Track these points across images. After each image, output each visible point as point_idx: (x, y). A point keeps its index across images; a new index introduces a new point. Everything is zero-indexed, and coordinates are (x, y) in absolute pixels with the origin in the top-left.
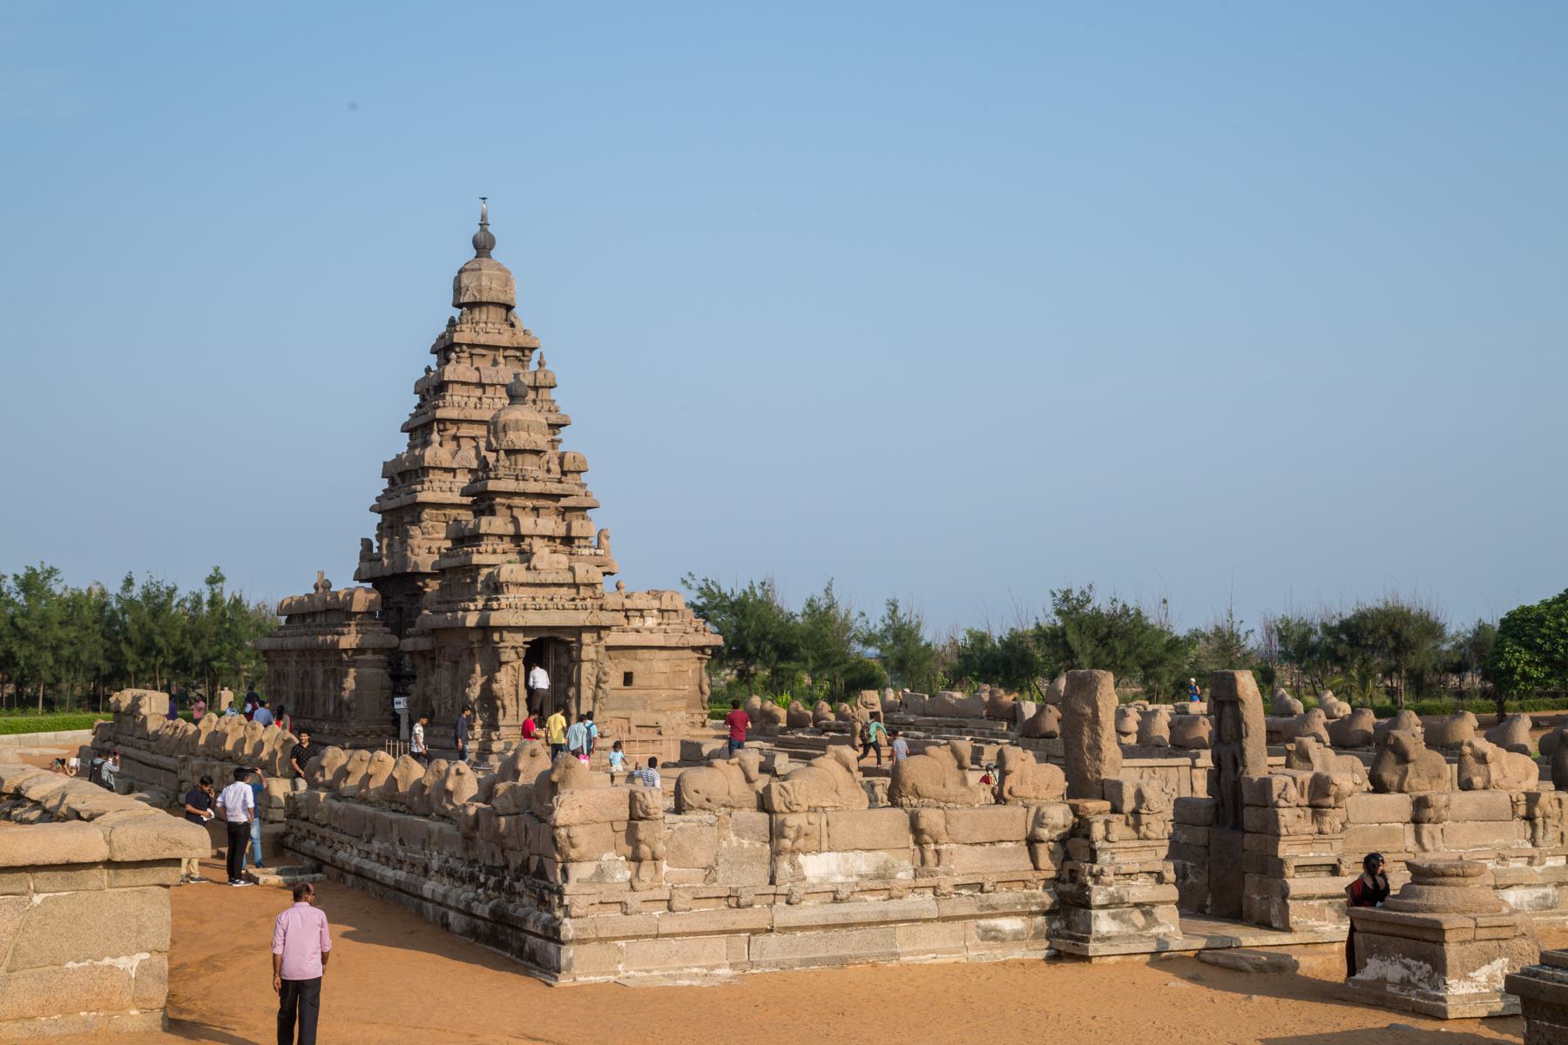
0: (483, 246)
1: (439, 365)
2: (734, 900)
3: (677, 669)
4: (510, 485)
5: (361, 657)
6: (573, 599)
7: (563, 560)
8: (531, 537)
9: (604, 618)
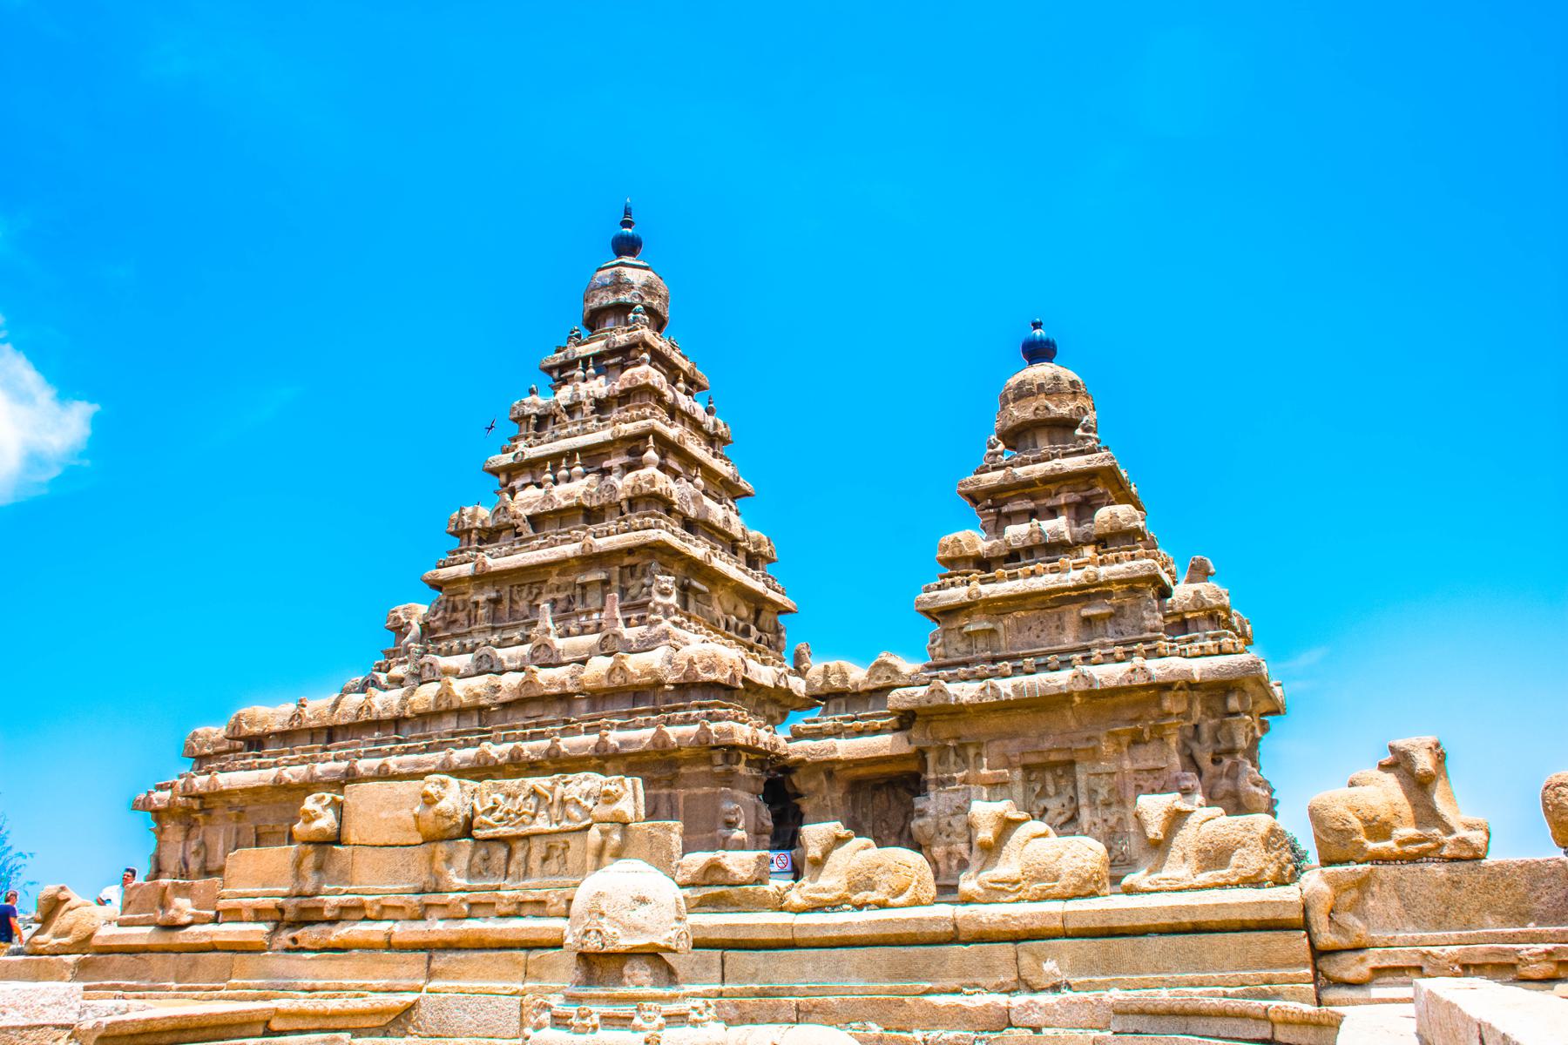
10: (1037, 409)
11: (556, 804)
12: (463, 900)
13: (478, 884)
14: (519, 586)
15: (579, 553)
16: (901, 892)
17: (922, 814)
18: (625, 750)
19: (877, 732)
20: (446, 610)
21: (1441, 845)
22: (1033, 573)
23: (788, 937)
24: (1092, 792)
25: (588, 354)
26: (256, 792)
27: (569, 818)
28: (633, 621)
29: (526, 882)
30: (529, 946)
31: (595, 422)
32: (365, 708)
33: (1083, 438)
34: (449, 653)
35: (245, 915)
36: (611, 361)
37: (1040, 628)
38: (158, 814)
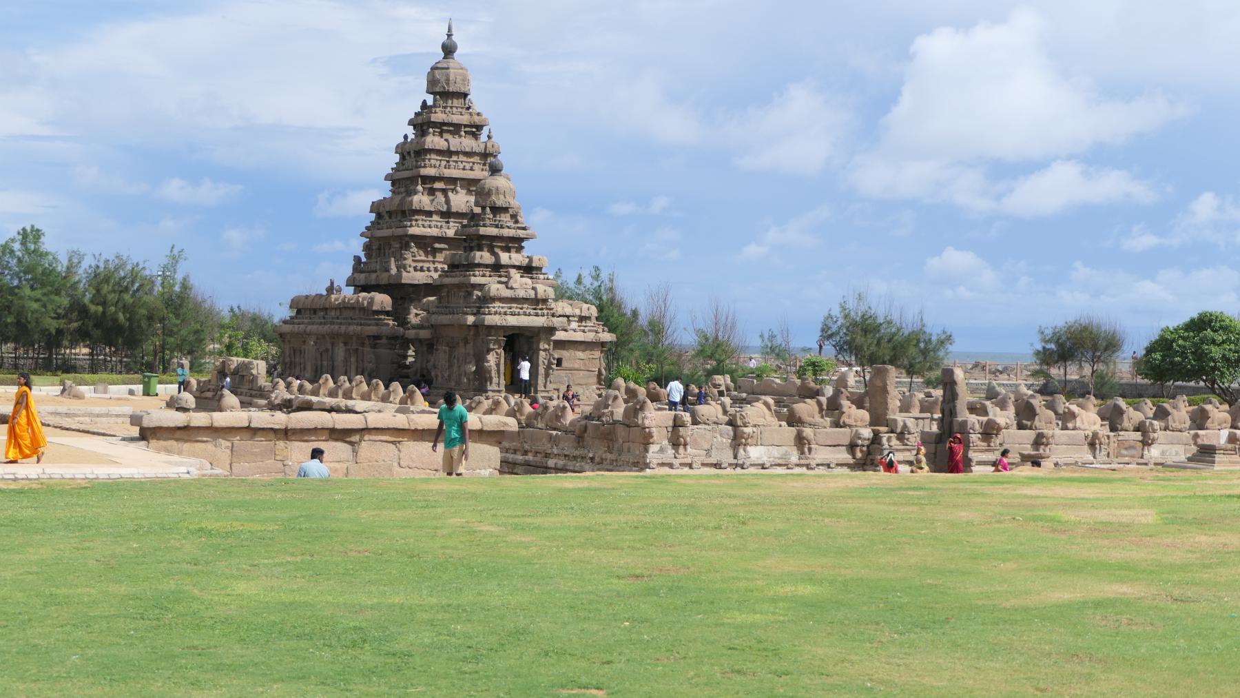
0: (449, 50)
2: (717, 466)
3: (591, 356)
4: (493, 231)
5: (378, 341)
6: (535, 309)
7: (529, 281)
8: (507, 266)
9: (557, 322)
20: (369, 249)
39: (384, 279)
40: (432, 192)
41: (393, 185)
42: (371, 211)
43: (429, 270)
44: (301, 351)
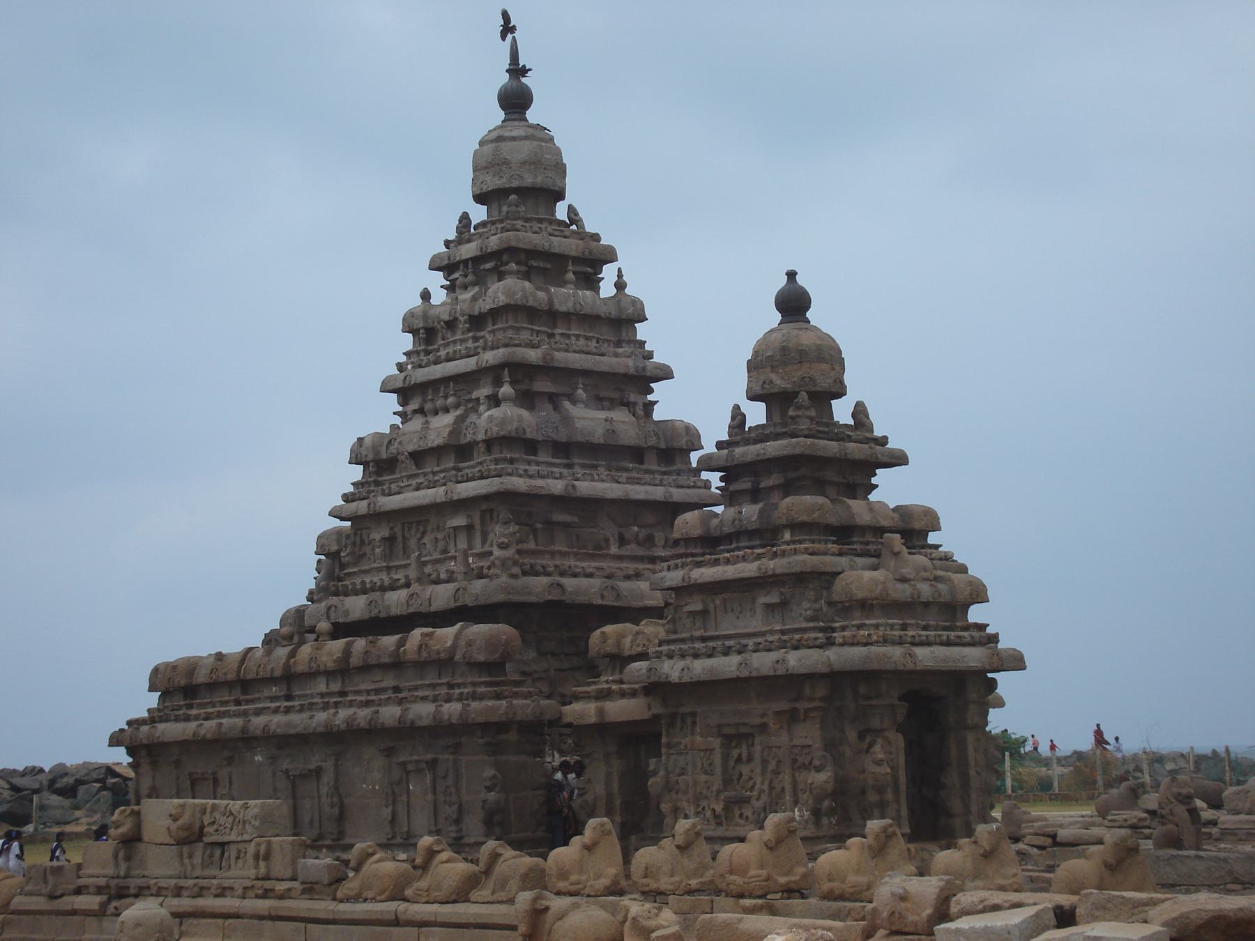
1: (451, 289)
5: (502, 737)
8: (864, 529)
10: (764, 383)
11: (241, 822)
12: (195, 885)
13: (207, 872)
14: (410, 523)
15: (443, 499)
16: (381, 893)
17: (655, 773)
18: (419, 723)
19: (633, 694)
21: (586, 887)
22: (728, 561)
23: (331, 917)
24: (765, 762)
25: (469, 256)
26: (185, 745)
27: (247, 832)
28: (485, 571)
29: (229, 874)
30: (227, 916)
31: (470, 344)
32: (262, 666)
33: (793, 418)
34: (356, 593)
35: (92, 890)
36: (488, 266)
37: (739, 610)
38: (131, 752)
39: (441, 596)
40: (527, 399)
41: (404, 402)
42: (355, 460)
43: (548, 574)
44: (216, 782)
